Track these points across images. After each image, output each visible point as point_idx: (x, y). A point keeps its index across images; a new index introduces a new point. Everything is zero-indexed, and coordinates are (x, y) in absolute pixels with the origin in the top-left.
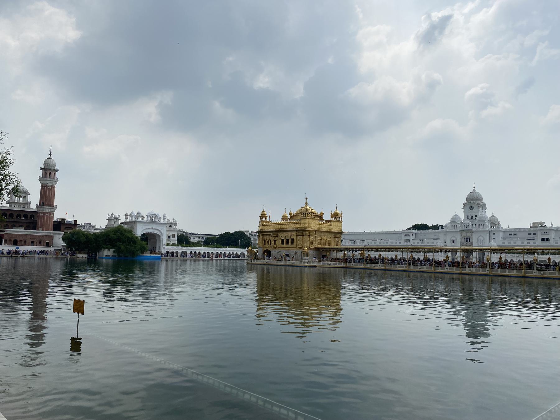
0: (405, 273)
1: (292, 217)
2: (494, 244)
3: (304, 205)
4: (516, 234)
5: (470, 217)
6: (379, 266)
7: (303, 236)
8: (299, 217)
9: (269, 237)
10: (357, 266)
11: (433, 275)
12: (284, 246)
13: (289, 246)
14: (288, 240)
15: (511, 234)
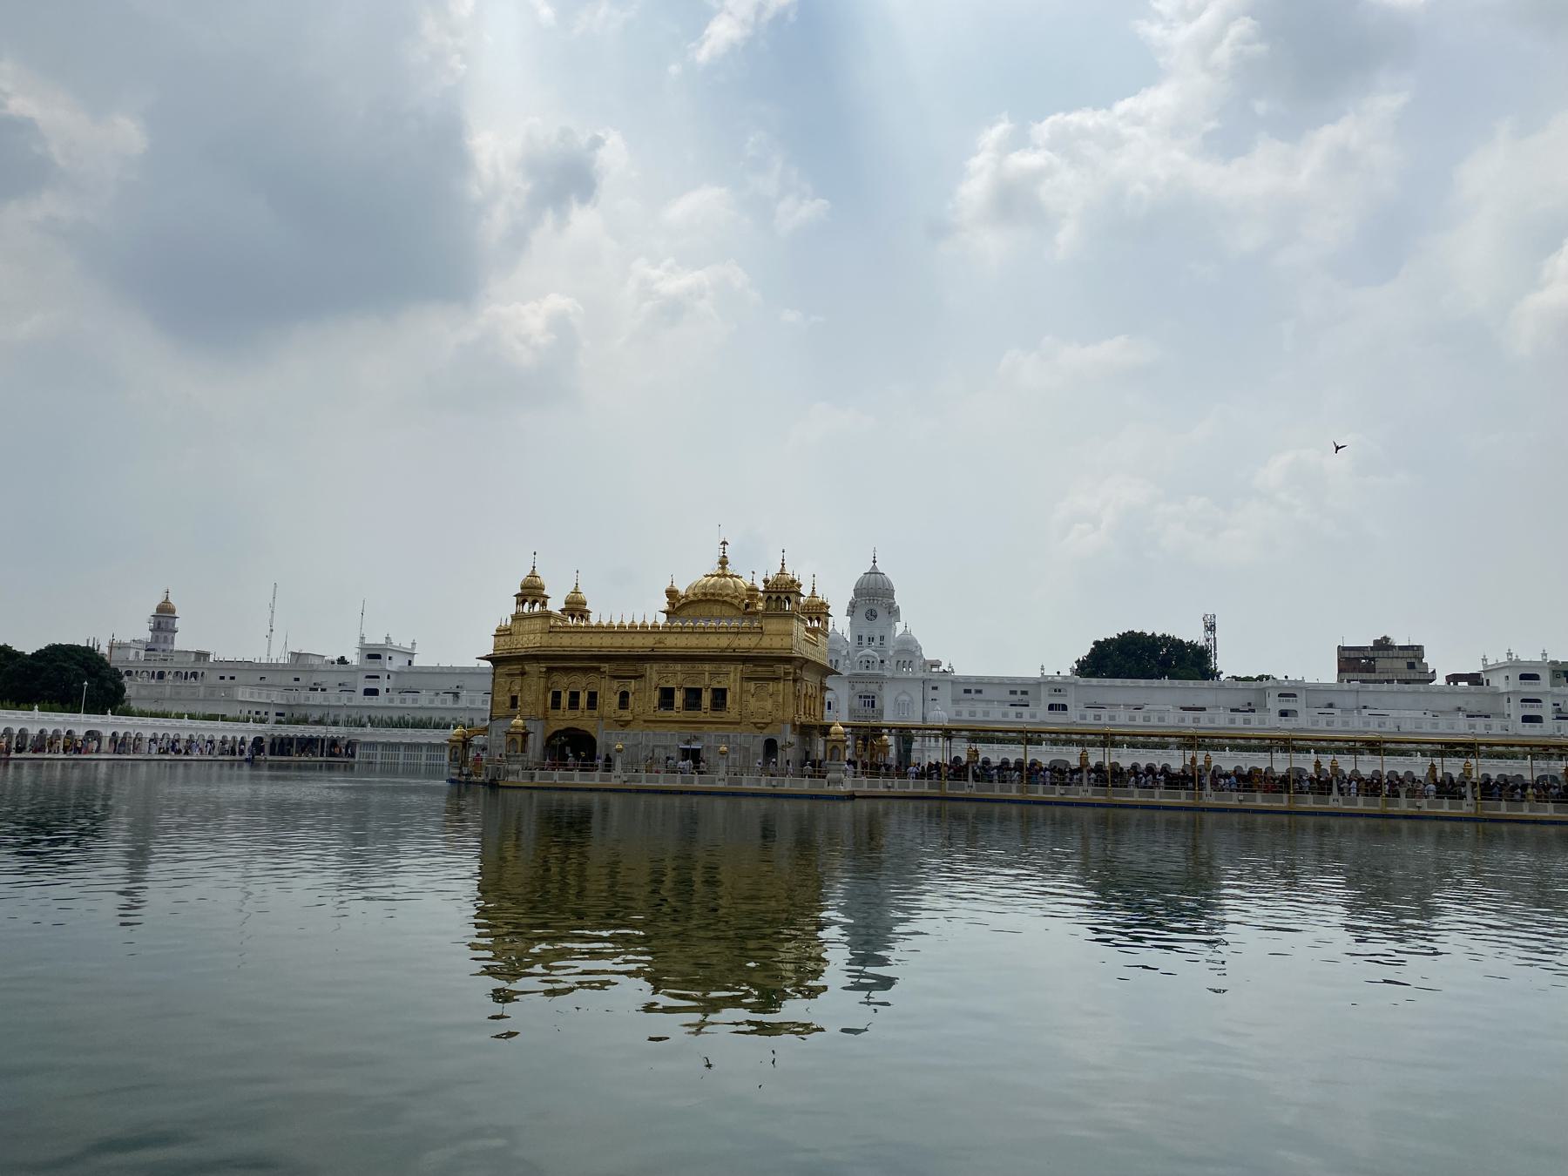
0: (1183, 816)
1: (678, 605)
2: (941, 714)
3: (716, 569)
4: (979, 692)
5: (865, 641)
6: (1085, 792)
7: (777, 679)
8: (716, 610)
9: (581, 683)
10: (988, 794)
11: (1285, 818)
12: (672, 715)
13: (701, 716)
14: (693, 697)
15: (967, 691)
